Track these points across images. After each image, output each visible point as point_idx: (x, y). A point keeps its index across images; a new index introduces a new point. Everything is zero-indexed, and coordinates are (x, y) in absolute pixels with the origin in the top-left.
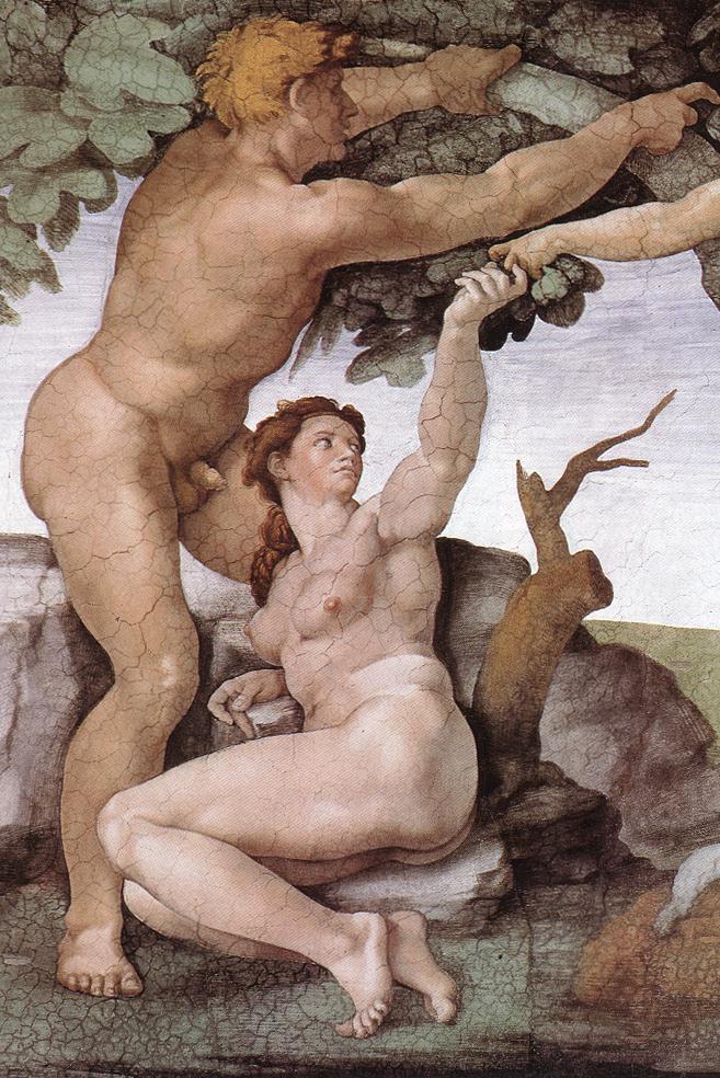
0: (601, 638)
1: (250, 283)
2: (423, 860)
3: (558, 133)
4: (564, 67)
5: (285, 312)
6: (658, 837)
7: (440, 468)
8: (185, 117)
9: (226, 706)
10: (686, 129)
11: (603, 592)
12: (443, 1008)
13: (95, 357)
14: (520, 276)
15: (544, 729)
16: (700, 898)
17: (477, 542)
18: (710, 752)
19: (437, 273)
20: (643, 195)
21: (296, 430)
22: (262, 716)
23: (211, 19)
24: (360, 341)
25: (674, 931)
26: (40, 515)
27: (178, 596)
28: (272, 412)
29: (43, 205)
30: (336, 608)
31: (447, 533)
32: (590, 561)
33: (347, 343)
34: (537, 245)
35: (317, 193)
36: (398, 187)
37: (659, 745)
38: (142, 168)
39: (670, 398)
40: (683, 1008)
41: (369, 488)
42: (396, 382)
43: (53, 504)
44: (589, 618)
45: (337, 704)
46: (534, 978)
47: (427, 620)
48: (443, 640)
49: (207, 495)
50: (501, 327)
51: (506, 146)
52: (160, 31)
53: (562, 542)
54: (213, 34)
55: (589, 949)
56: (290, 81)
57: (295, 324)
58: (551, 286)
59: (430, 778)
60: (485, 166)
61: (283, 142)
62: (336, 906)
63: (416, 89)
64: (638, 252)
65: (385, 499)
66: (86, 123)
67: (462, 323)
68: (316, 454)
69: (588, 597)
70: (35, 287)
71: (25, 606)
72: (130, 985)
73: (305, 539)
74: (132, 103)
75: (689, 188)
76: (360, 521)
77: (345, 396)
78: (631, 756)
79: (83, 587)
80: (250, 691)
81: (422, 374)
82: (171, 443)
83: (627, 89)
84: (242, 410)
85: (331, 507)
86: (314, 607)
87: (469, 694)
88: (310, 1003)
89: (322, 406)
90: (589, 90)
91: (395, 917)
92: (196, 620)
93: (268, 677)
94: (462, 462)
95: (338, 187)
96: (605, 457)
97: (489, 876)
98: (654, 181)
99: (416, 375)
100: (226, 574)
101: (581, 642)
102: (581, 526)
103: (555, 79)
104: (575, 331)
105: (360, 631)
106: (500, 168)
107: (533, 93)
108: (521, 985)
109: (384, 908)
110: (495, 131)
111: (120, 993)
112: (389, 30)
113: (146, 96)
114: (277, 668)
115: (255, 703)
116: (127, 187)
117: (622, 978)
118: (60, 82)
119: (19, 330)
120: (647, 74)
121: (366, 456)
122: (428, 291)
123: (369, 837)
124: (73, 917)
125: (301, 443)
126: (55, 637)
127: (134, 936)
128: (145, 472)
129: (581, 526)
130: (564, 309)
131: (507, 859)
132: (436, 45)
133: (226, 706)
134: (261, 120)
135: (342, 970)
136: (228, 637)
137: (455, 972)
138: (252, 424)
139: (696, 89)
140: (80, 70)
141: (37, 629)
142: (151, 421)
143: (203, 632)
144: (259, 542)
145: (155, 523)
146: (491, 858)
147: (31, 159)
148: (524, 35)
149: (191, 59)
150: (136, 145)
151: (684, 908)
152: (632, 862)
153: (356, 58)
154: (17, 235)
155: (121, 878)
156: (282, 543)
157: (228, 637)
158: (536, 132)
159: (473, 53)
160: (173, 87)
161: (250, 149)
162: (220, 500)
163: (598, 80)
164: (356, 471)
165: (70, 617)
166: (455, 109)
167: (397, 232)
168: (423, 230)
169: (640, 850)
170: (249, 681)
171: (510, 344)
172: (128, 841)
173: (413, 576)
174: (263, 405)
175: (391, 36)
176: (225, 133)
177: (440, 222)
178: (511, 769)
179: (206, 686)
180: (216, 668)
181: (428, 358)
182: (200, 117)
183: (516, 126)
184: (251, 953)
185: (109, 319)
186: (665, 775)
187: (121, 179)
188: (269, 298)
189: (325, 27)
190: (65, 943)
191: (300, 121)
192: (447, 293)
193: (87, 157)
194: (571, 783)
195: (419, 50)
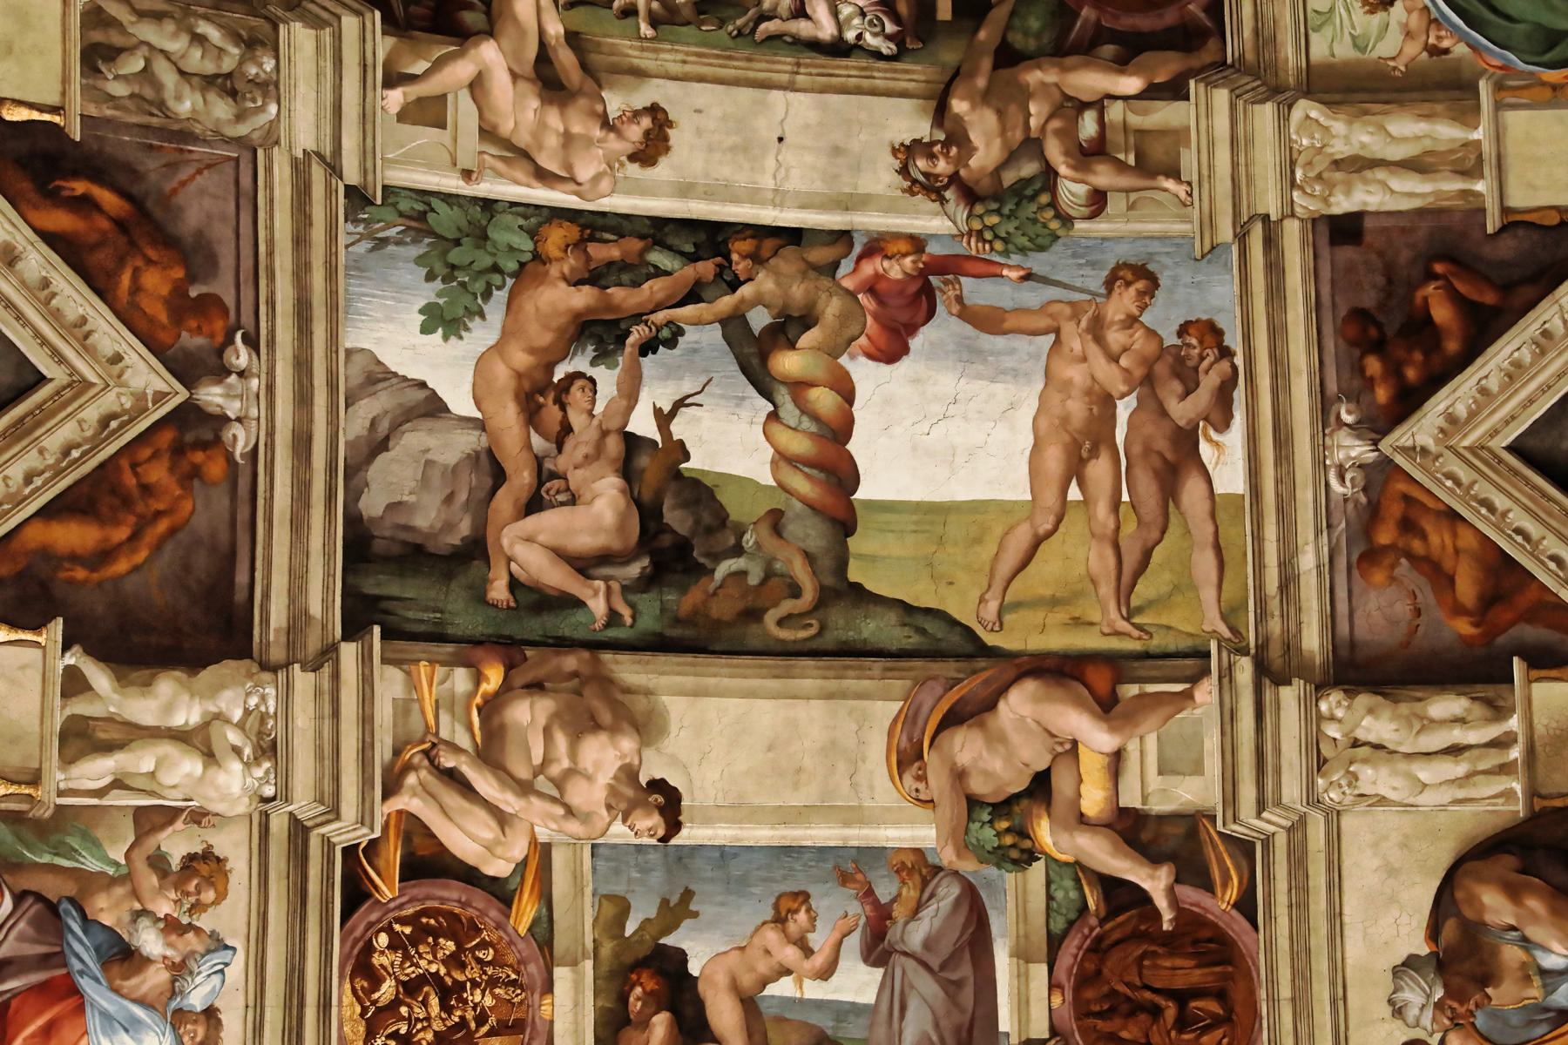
0: (686, 474)
1: (555, 324)
2: (619, 560)
3: (667, 273)
4: (670, 248)
5: (568, 336)
6: (708, 555)
7: (624, 403)
8: (528, 257)
9: (547, 492)
10: (715, 275)
11: (687, 457)
12: (629, 621)
13: (498, 348)
14: (654, 328)
15: (664, 511)
16: (724, 580)
17: (639, 433)
18: (728, 523)
19: (623, 326)
20: (699, 300)
21: (572, 384)
22: (561, 498)
23: (541, 219)
24: (595, 350)
25: (715, 594)
26: (479, 409)
27: (528, 446)
28: (562, 376)
29: (479, 286)
30: (586, 457)
31: (628, 429)
32: (681, 443)
33: (590, 350)
34: (660, 316)
35: (580, 291)
36: (609, 291)
37: (707, 518)
38: (516, 275)
39: (710, 380)
40: (718, 624)
41: (599, 408)
42: (608, 368)
43: (483, 407)
44: (683, 466)
45: (587, 496)
46: (663, 610)
47: (620, 464)
48: (627, 471)
49: (540, 407)
50: (647, 348)
51: (649, 277)
52: (521, 221)
53: (670, 434)
54: (540, 225)
55: (683, 599)
56: (568, 246)
57: (571, 341)
58: (665, 333)
59: (621, 528)
60: (640, 285)
61: (566, 270)
62: (589, 577)
63: (614, 252)
64: (698, 322)
65: (604, 413)
66: (494, 255)
67: (632, 346)
68: (579, 394)
69: (681, 457)
70: (477, 318)
71: (474, 446)
72: (512, 604)
73: (576, 428)
74: (511, 249)
75: (717, 298)
76: (595, 422)
77: (590, 372)
78: (697, 522)
79: (494, 438)
80: (556, 487)
81: (617, 365)
82: (527, 385)
83: (693, 258)
84: (552, 374)
85: (584, 416)
86: (579, 454)
87: (636, 493)
88: (579, 616)
89: (579, 375)
90: (678, 256)
91: (611, 583)
92: (536, 457)
93: (562, 482)
94: (633, 401)
95: (586, 289)
96: (688, 401)
97: (644, 568)
98: (704, 295)
99: (615, 365)
100: (546, 438)
101: (678, 475)
102: (678, 429)
103: (666, 252)
104: (676, 351)
105: (596, 467)
106: (646, 286)
107: (658, 258)
108: (658, 612)
109: (606, 579)
110: (644, 271)
111: (509, 607)
112: (605, 229)
113: (516, 246)
114: (566, 479)
115: (558, 492)
116: (510, 282)
117: (695, 612)
118: (486, 238)
119: (473, 335)
120: (701, 253)
121: (598, 396)
122: (619, 333)
123: (600, 549)
124: (491, 575)
125: (574, 389)
126: (484, 459)
127: (514, 584)
128: (517, 397)
129: (678, 429)
130: (671, 343)
131: (652, 562)
132: (622, 236)
133: (547, 492)
134: (557, 260)
135: (591, 603)
136: (548, 465)
137: (632, 606)
138: (555, 380)
139: (719, 259)
140: (494, 234)
141: (477, 454)
142: (519, 376)
143: (539, 461)
144: (557, 428)
145: (521, 417)
146: (646, 562)
147: (476, 267)
148: (653, 236)
149: (533, 234)
150: (511, 266)
151: (718, 583)
152: (702, 566)
153: (592, 239)
154: (471, 297)
155: (509, 560)
156: (566, 429)
157: (548, 465)
158: (659, 273)
159: (636, 240)
160: (526, 245)
161: (554, 270)
162: (544, 409)
163: (682, 254)
164: (593, 402)
165: (490, 452)
166: (628, 261)
167: (610, 307)
168: (617, 308)
169: (702, 560)
170: (556, 484)
171: (650, 356)
172: (511, 545)
173: (614, 445)
174: (559, 373)
175: (606, 231)
176: (545, 264)
177: (625, 305)
178: (652, 526)
179: (540, 484)
180: (544, 477)
181: (620, 359)
182: (537, 257)
183: (652, 270)
184: (555, 593)
185: (506, 334)
186: (709, 531)
187: (508, 279)
188: (561, 331)
189: (579, 226)
190: (488, 586)
191: (572, 261)
192: (628, 333)
193: (496, 269)
194: (673, 532)
195: (615, 238)
